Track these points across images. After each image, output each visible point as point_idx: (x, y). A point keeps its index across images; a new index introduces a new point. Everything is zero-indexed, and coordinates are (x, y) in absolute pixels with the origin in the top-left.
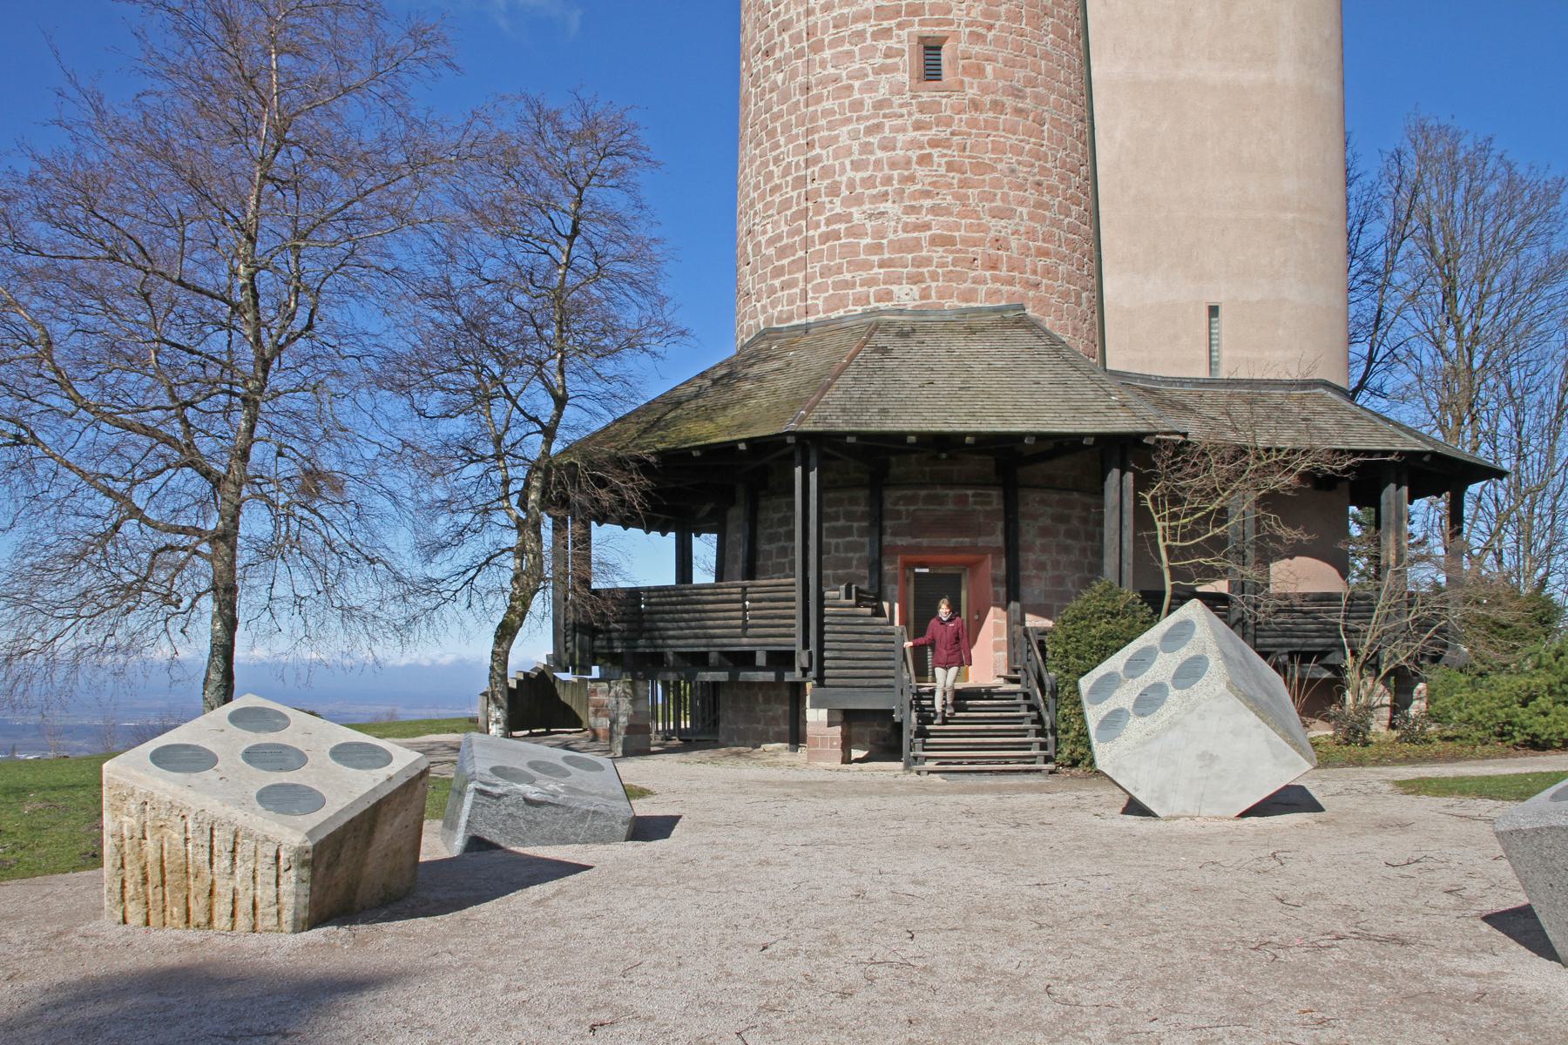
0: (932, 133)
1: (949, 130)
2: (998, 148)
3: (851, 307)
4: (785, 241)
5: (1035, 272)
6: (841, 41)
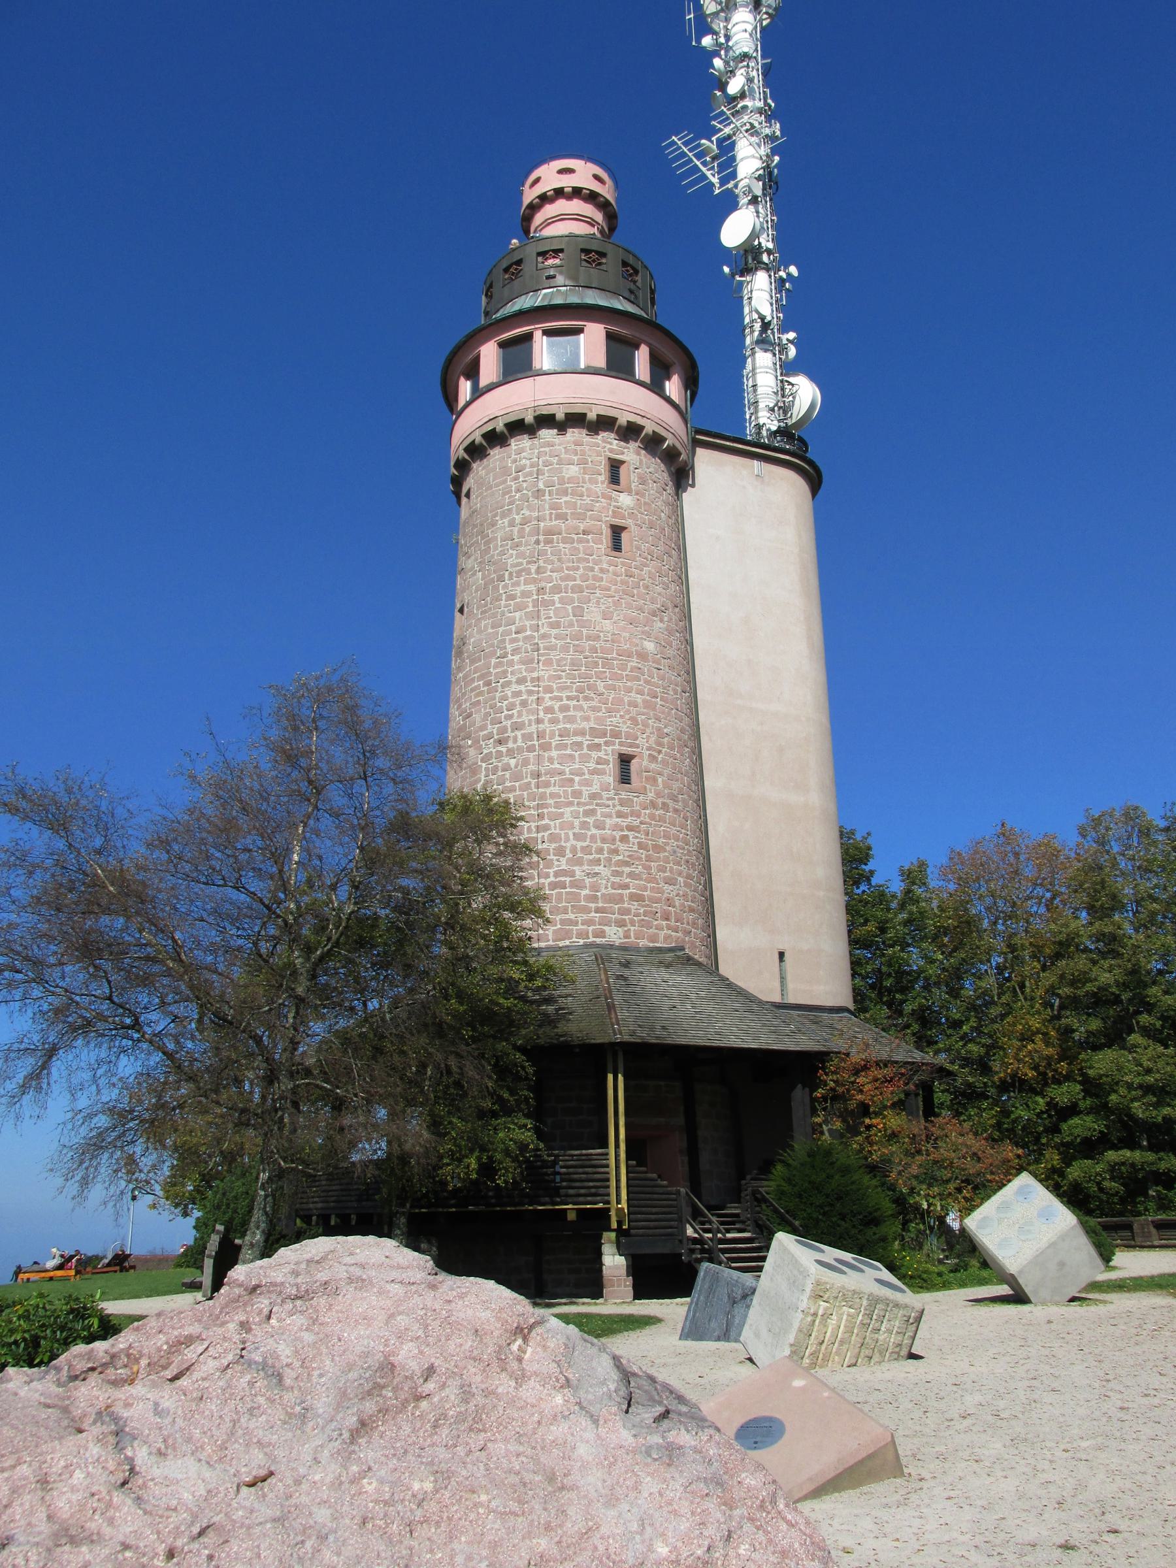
3: (574, 940)
6: (565, 747)
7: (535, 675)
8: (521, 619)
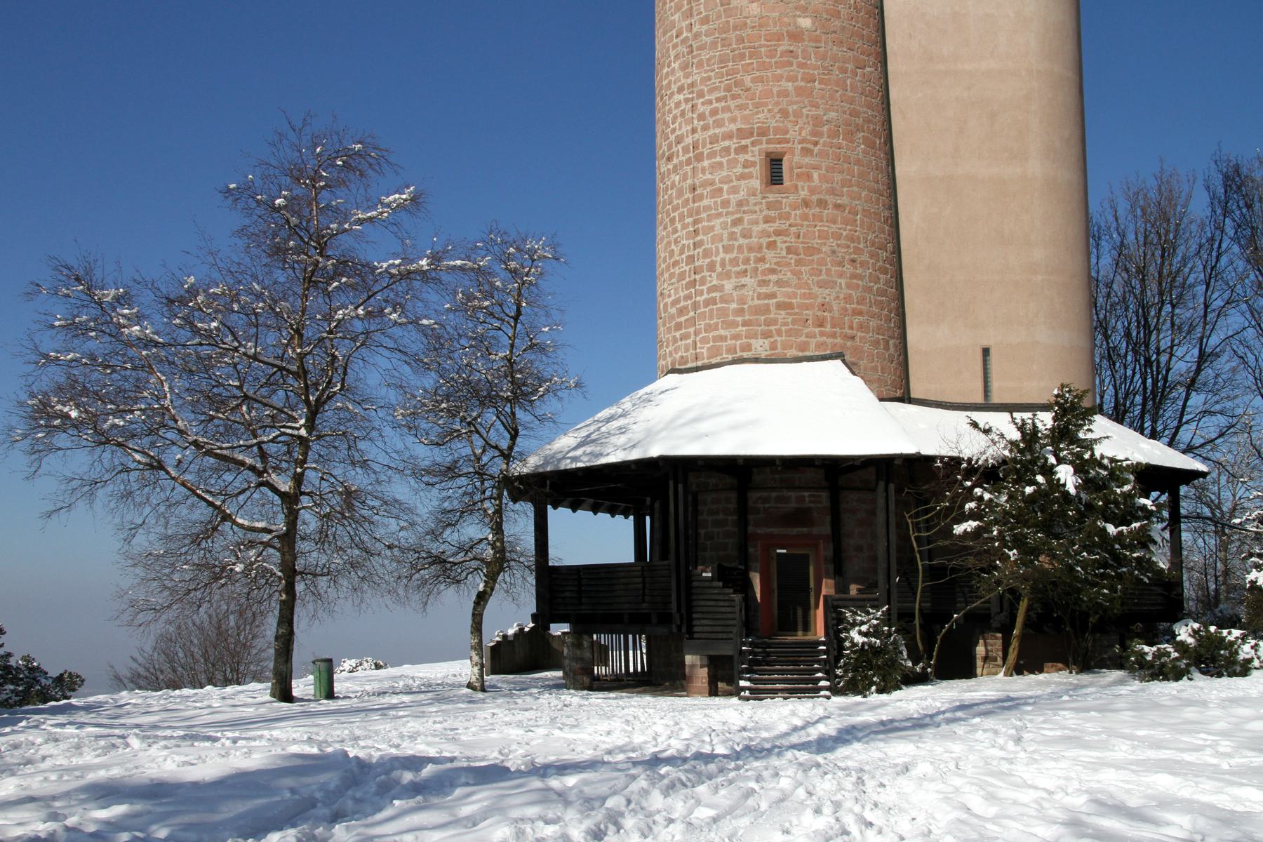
0: (776, 225)
1: (788, 223)
2: (824, 237)
3: (724, 356)
4: (682, 304)
5: (851, 328)
7: (689, 81)
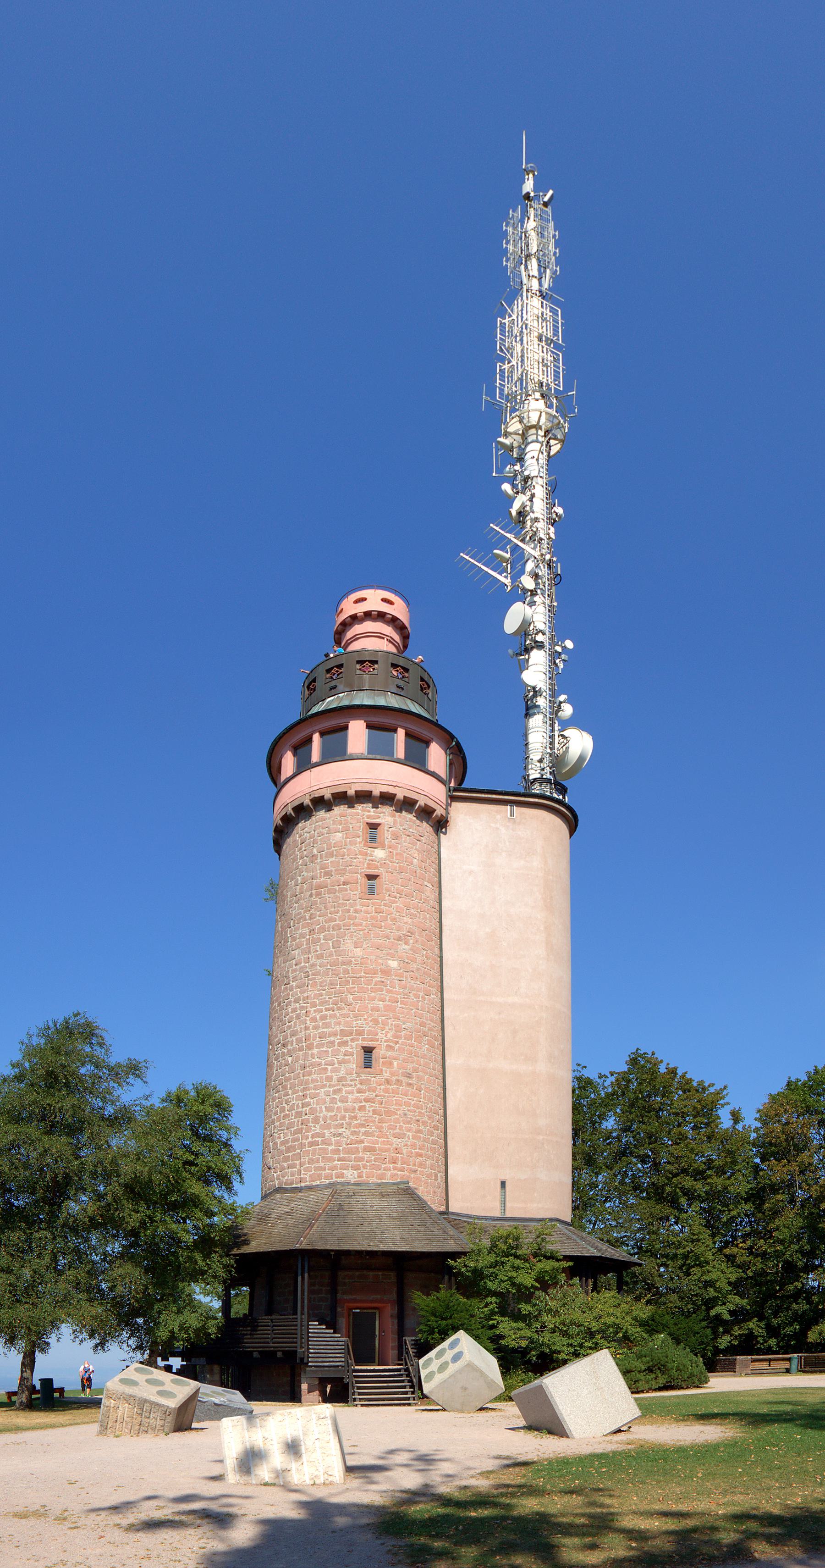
1: (374, 1094)
3: (323, 1180)
7: (305, 995)
8: (299, 954)
